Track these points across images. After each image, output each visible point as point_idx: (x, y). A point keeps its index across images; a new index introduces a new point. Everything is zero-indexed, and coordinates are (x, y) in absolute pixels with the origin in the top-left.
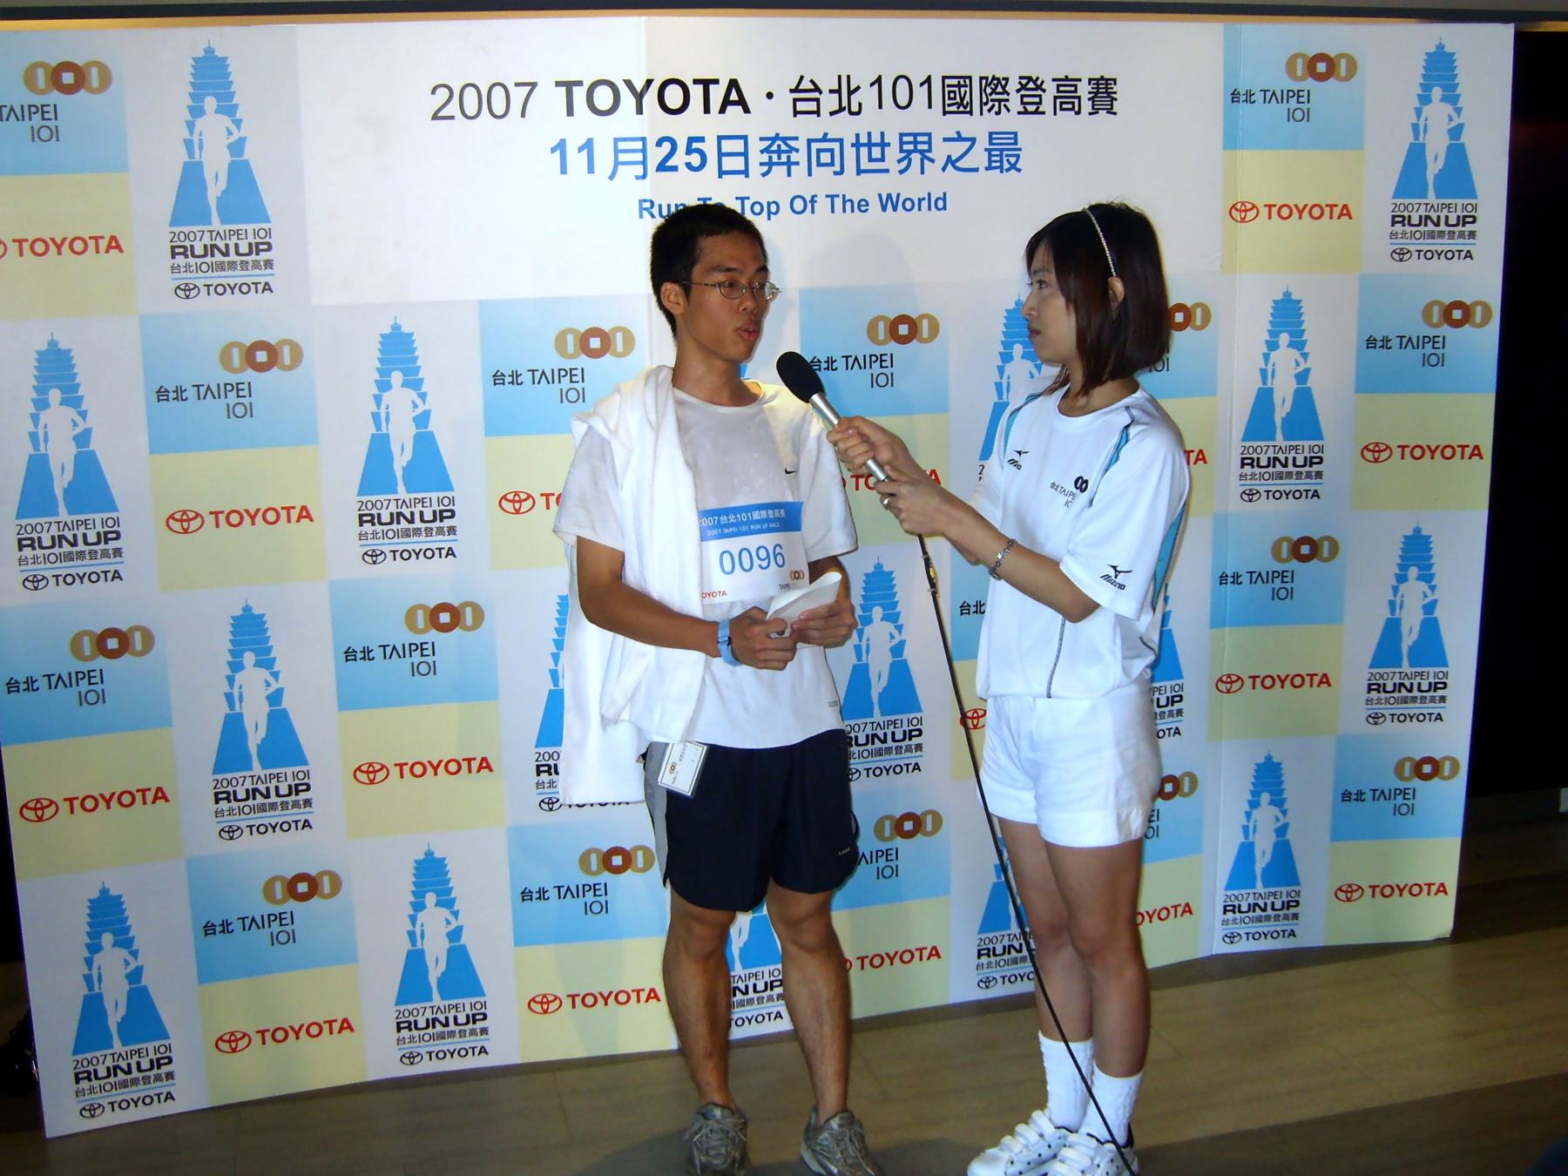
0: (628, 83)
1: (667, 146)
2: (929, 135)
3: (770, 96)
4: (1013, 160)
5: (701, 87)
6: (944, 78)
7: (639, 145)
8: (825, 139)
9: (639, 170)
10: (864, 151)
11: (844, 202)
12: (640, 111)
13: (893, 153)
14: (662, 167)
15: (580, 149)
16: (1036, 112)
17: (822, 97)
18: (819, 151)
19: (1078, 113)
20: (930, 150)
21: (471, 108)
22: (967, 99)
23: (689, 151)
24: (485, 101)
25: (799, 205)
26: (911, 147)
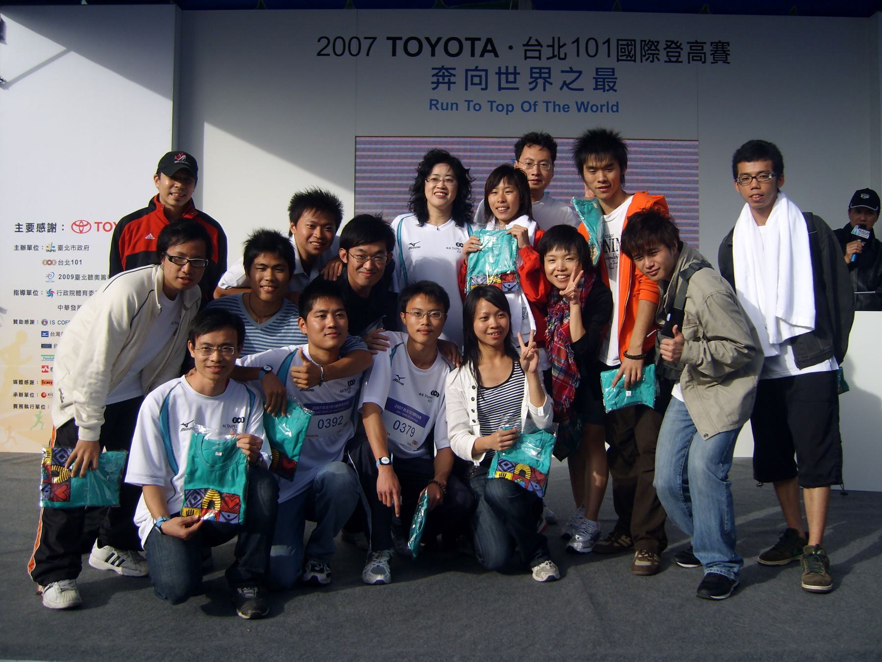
0: (428, 39)
3: (511, 48)
5: (470, 42)
6: (618, 40)
12: (433, 54)
16: (677, 61)
17: (542, 49)
22: (633, 53)
25: (526, 106)
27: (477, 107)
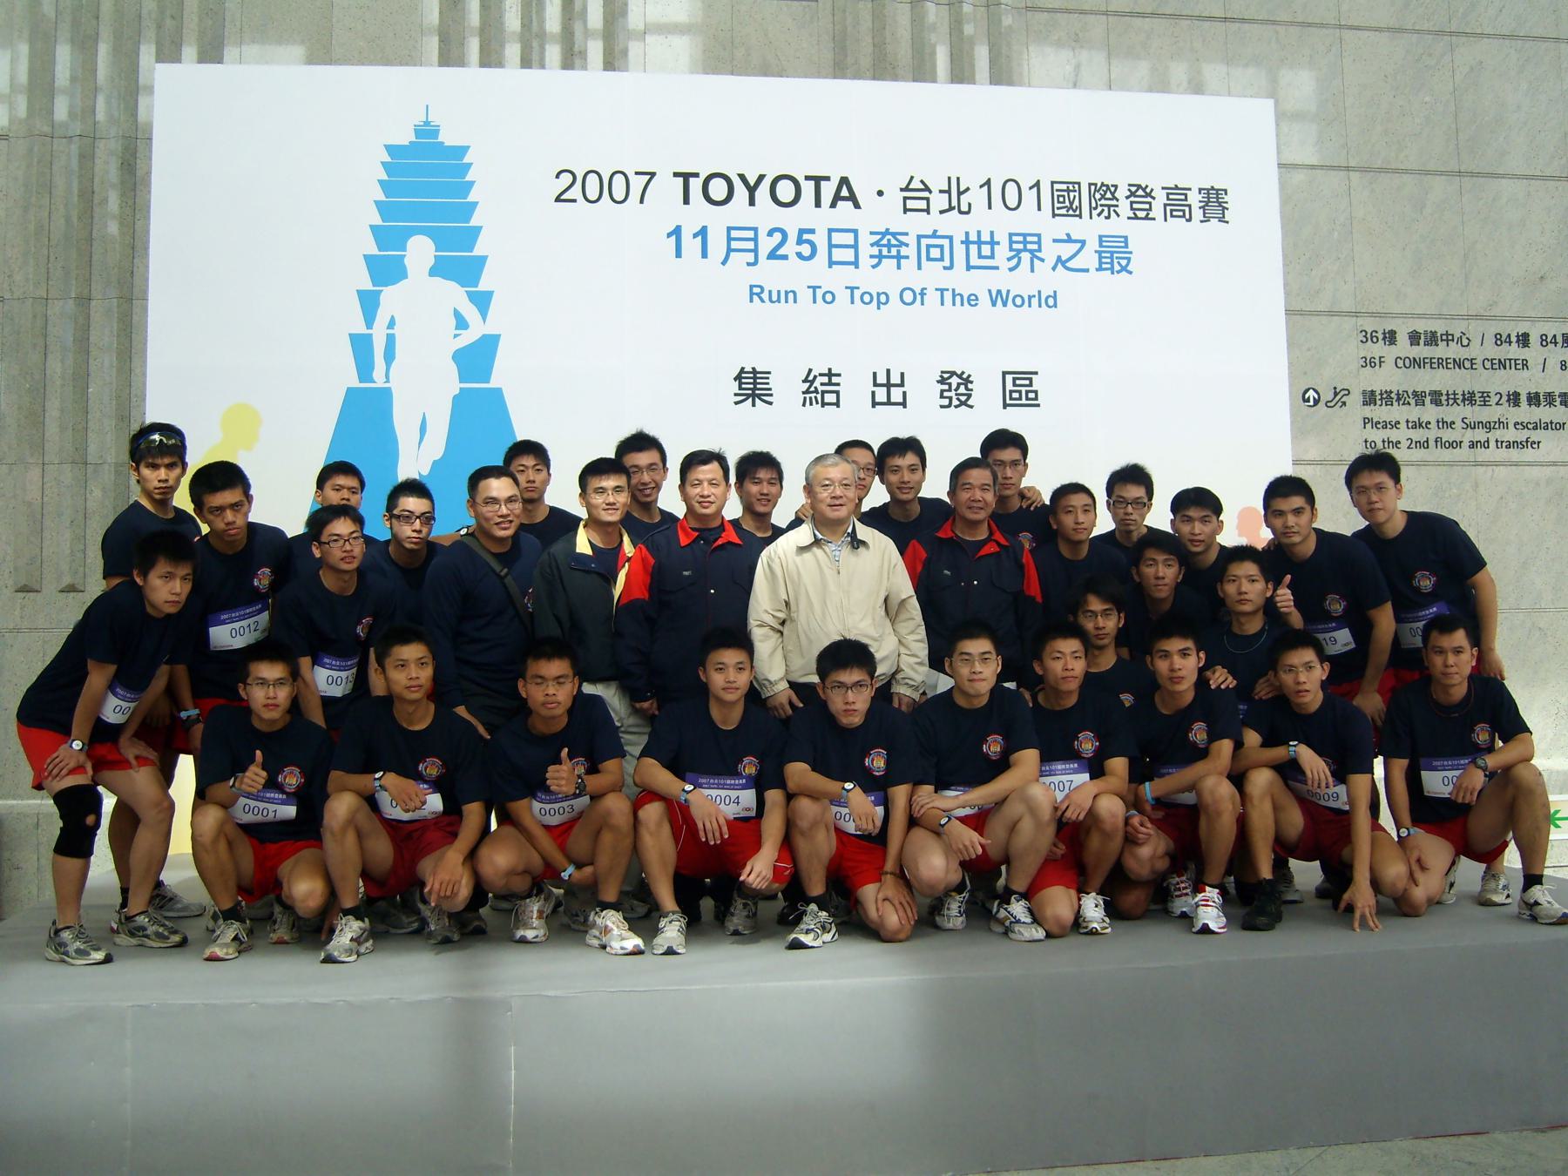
0: (742, 177)
1: (778, 237)
2: (1039, 236)
4: (1124, 262)
7: (751, 234)
8: (934, 235)
9: (750, 257)
10: (973, 248)
11: (954, 296)
12: (752, 202)
13: (1002, 251)
14: (772, 255)
15: (695, 236)
16: (1147, 218)
18: (928, 247)
19: (1189, 220)
20: (1039, 250)
21: (592, 195)
22: (1076, 203)
23: (800, 242)
24: (606, 187)
25: (908, 296)
26: (1021, 246)
27: (829, 297)
